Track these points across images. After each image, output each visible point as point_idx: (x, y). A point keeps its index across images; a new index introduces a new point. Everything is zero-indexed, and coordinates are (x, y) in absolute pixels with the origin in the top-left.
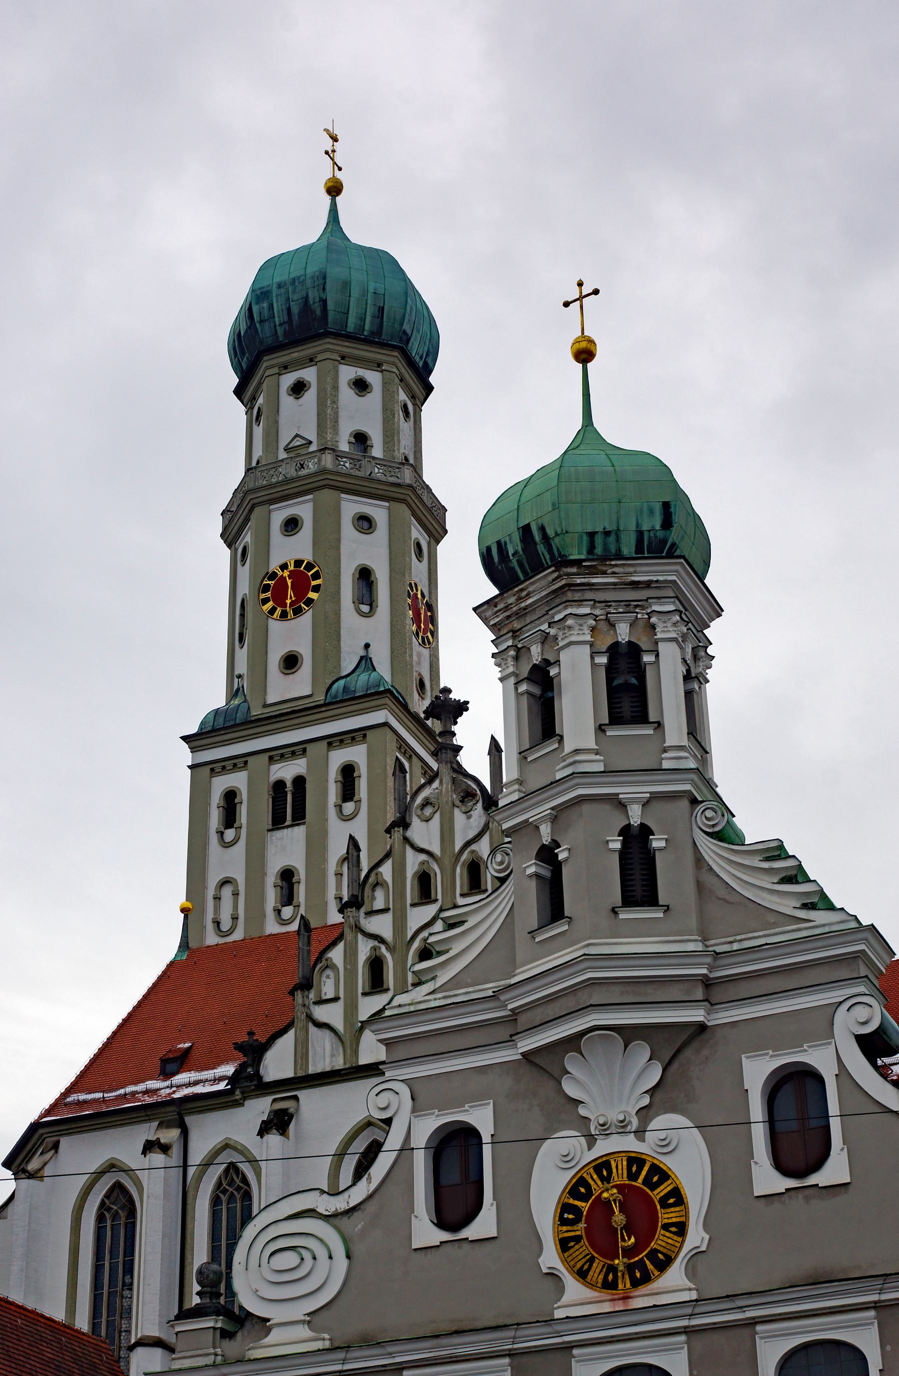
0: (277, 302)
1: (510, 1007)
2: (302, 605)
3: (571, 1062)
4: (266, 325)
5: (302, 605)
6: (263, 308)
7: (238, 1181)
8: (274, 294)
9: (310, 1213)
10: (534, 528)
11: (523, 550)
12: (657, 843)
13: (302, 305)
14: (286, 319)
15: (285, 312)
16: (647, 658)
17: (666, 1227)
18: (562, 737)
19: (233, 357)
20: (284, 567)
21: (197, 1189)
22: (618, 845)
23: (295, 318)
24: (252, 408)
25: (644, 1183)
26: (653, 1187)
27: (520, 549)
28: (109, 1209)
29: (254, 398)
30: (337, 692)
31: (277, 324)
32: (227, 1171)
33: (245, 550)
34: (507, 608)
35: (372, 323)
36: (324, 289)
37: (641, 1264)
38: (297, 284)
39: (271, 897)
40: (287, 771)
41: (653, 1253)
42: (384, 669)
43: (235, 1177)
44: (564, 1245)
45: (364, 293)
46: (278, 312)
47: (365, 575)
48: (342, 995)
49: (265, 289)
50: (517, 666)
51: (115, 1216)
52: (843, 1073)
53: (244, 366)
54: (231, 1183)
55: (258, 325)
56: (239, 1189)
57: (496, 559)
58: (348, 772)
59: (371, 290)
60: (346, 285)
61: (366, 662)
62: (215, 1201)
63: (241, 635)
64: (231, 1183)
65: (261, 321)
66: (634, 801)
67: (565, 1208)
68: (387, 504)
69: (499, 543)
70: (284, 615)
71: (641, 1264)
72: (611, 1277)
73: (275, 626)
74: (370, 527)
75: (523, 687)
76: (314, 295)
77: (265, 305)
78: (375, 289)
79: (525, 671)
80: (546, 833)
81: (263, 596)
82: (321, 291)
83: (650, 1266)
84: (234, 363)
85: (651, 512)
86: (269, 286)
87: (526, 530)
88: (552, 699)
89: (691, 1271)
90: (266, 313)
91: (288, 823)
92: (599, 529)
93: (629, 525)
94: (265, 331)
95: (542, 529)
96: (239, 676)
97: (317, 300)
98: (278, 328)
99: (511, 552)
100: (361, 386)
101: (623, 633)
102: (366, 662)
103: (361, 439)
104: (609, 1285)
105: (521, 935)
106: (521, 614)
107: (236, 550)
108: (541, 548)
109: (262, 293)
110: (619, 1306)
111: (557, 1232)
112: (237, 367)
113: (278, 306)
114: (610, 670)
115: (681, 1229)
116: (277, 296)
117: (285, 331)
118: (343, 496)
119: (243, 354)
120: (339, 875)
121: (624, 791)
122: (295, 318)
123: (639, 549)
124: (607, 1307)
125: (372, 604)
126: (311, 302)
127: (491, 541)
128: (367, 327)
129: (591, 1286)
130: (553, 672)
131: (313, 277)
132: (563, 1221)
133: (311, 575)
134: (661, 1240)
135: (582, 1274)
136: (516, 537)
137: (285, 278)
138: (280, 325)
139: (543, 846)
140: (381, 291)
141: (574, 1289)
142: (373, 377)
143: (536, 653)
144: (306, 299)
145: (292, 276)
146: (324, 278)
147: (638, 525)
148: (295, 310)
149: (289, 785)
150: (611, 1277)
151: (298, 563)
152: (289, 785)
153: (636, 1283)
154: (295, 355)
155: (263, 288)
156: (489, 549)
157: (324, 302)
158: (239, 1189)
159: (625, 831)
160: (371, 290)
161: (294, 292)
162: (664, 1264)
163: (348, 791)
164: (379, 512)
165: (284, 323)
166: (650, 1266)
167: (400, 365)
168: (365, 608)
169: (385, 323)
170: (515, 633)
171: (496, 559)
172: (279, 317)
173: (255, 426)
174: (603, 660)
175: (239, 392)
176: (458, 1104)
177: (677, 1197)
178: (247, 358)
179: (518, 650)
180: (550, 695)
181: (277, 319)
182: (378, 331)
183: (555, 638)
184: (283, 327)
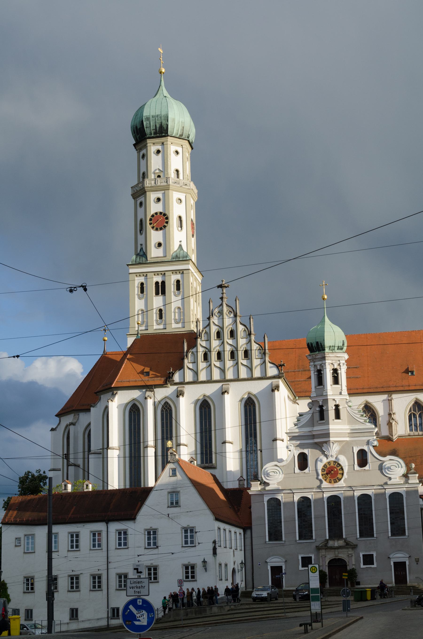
0: (152, 122)
1: (313, 434)
2: (163, 227)
3: (324, 445)
4: (148, 129)
5: (163, 227)
6: (147, 123)
7: (168, 406)
8: (151, 119)
9: (276, 465)
10: (319, 342)
11: (317, 346)
12: (340, 407)
13: (160, 125)
14: (154, 128)
15: (155, 126)
16: (339, 372)
17: (340, 474)
18: (324, 386)
19: (133, 134)
20: (156, 213)
21: (157, 408)
22: (334, 408)
23: (158, 129)
24: (140, 152)
25: (336, 466)
26: (338, 467)
27: (316, 345)
28: (132, 410)
29: (141, 149)
30: (174, 257)
31: (152, 129)
32: (165, 403)
33: (141, 204)
34: (312, 357)
35: (180, 132)
36: (168, 121)
37: (335, 480)
38: (158, 117)
39: (155, 316)
40: (159, 279)
41: (338, 478)
42: (185, 249)
43: (167, 405)
44: (322, 475)
45: (179, 122)
46: (152, 126)
47: (180, 217)
48: (196, 361)
49: (148, 117)
50: (314, 369)
51: (134, 412)
52: (371, 452)
53: (138, 138)
54: (166, 407)
55: (145, 129)
56: (168, 408)
57: (310, 346)
58: (178, 282)
59: (181, 121)
60: (174, 120)
61: (180, 246)
62: (162, 411)
63: (141, 230)
64: (166, 407)
65: (146, 128)
66: (337, 400)
67: (323, 469)
68: (185, 195)
69: (311, 343)
70: (157, 229)
71: (335, 480)
72: (330, 481)
73: (153, 232)
74: (181, 202)
75: (316, 373)
76: (164, 122)
77: (148, 122)
78: (182, 121)
79: (316, 370)
80: (321, 403)
81: (150, 222)
82: (167, 122)
83: (337, 480)
84: (133, 135)
85: (341, 342)
86: (149, 116)
87: (317, 343)
88: (322, 377)
89: (345, 481)
90: (148, 125)
91: (159, 295)
92: (332, 345)
93: (337, 345)
94: (147, 131)
95: (321, 344)
96: (141, 245)
97: (165, 124)
98: (152, 130)
99: (314, 346)
100: (177, 152)
101: (336, 366)
102: (180, 246)
103: (177, 171)
104: (330, 482)
105: (315, 421)
106: (316, 359)
107: (137, 201)
108: (320, 347)
109: (147, 118)
110: (332, 486)
111: (321, 473)
112: (136, 139)
113: (152, 123)
114: (333, 373)
115: (343, 474)
116: (152, 120)
117: (154, 132)
118: (174, 192)
119: (138, 134)
120: (175, 313)
121: (335, 397)
122: (158, 129)
123: (338, 349)
124: (330, 486)
125: (181, 227)
126: (163, 125)
127: (310, 342)
128: (179, 133)
129: (327, 482)
130: (322, 372)
131: (164, 116)
132: (322, 471)
133: (165, 218)
134: (339, 476)
135: (326, 480)
136: (315, 343)
137: (154, 114)
138: (153, 130)
139: (320, 405)
140: (183, 121)
141: (324, 482)
142: (180, 150)
143: (319, 368)
144: (161, 123)
145: (157, 114)
146: (168, 117)
147: (338, 345)
148: (158, 126)
149: (160, 284)
150: (330, 481)
151: (161, 213)
152: (160, 284)
153: (335, 482)
154: (157, 141)
155: (147, 116)
156: (309, 343)
157: (168, 125)
158: (168, 408)
159: (335, 405)
160: (181, 121)
161: (158, 120)
162: (340, 480)
163: (178, 288)
164: (182, 196)
165: (154, 129)
166: (337, 480)
167: (188, 146)
168: (180, 229)
169: (184, 132)
170: (314, 362)
171: (310, 346)
172: (152, 127)
173: (141, 159)
174: (332, 371)
175: (134, 145)
176: (303, 449)
177: (342, 469)
178: (139, 136)
179: (314, 365)
180: (321, 376)
181: (151, 128)
182: (182, 135)
183: (323, 366)
184: (153, 131)
